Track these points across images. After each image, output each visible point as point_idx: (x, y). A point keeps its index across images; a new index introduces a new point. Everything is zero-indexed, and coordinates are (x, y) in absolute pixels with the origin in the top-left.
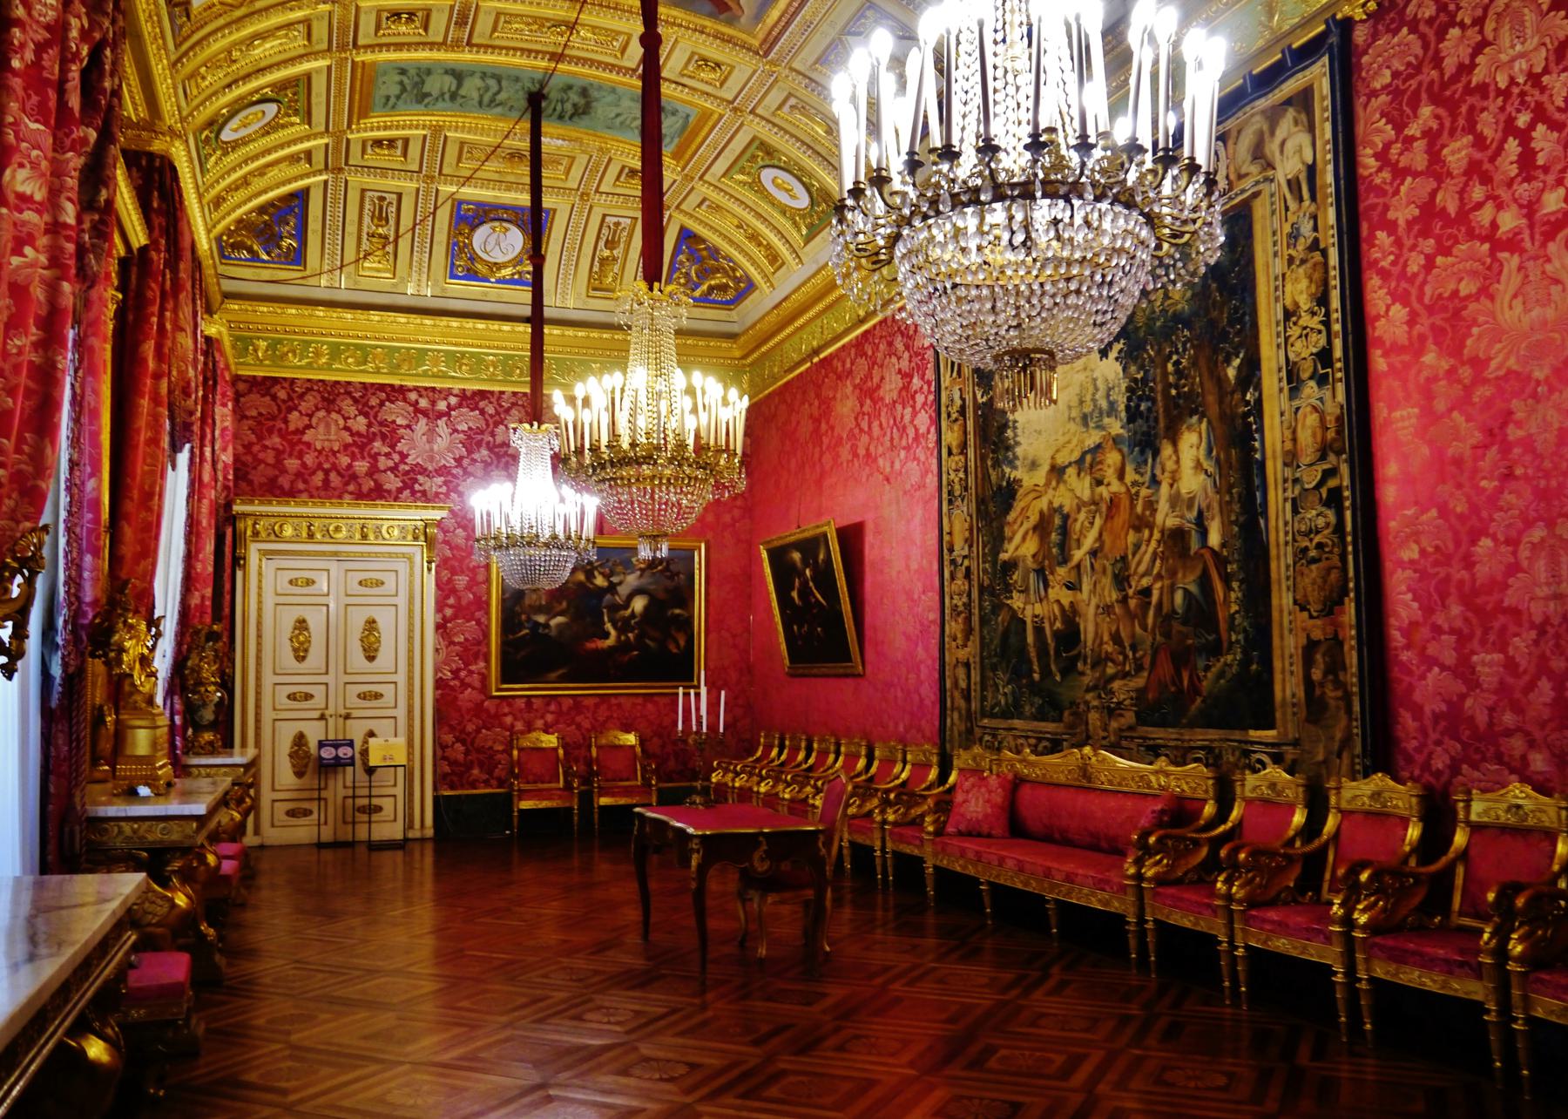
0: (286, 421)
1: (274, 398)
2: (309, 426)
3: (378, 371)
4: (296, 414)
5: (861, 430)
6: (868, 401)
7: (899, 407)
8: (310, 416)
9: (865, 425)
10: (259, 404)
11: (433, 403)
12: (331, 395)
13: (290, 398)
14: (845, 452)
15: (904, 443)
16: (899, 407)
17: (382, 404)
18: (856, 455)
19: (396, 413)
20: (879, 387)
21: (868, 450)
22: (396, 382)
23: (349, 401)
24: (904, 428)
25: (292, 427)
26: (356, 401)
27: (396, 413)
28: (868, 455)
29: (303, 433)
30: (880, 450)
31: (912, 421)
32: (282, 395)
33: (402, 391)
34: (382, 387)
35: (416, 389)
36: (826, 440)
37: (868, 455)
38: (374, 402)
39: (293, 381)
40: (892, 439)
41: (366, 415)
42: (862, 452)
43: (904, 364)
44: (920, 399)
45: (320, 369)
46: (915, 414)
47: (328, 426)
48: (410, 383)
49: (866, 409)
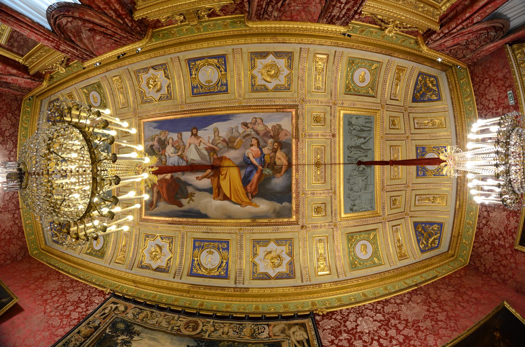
0: (9, 112)
1: (16, 110)
2: (7, 119)
3: (21, 140)
4: (11, 115)
5: (51, 294)
6: (61, 292)
7: (69, 304)
8: (10, 120)
9: (53, 294)
10: (15, 105)
11: (13, 156)
12: (15, 126)
13: (15, 115)
14: (40, 292)
15: (62, 312)
16: (69, 304)
17: (12, 141)
18: (42, 296)
19: (10, 145)
20: (68, 293)
21: (47, 299)
22: (18, 146)
23: (13, 131)
24: (66, 309)
25: (8, 114)
26: (13, 133)
27: (10, 145)
28: (46, 300)
29: (6, 117)
30: (51, 304)
31: (71, 311)
32: (16, 112)
33: (16, 147)
34: (17, 141)
35: (16, 151)
36: (38, 283)
37: (46, 300)
38: (13, 138)
39: (19, 116)
40: (58, 307)
41: (9, 136)
42: (45, 297)
43: (83, 298)
44: (79, 310)
45: (22, 124)
46: (74, 310)
47: (7, 124)
48: (18, 149)
49: (57, 292)
